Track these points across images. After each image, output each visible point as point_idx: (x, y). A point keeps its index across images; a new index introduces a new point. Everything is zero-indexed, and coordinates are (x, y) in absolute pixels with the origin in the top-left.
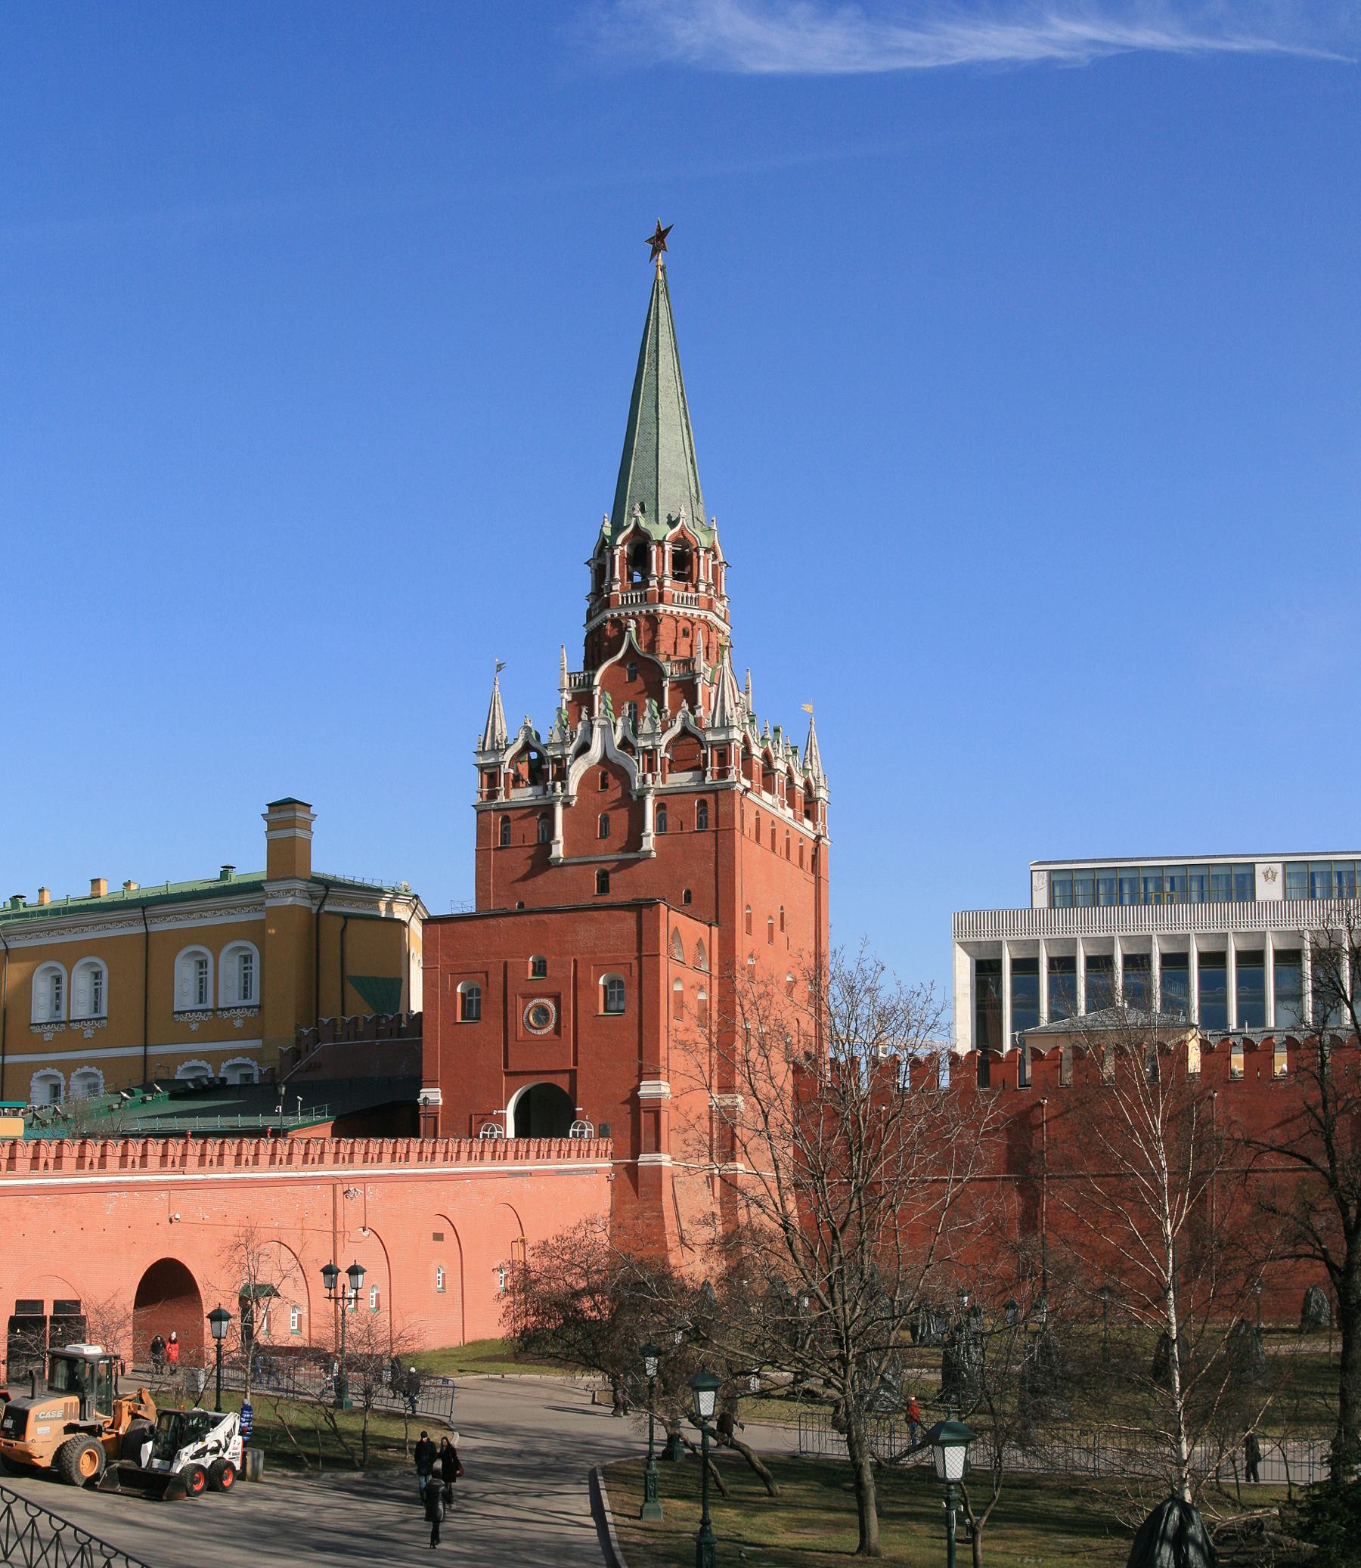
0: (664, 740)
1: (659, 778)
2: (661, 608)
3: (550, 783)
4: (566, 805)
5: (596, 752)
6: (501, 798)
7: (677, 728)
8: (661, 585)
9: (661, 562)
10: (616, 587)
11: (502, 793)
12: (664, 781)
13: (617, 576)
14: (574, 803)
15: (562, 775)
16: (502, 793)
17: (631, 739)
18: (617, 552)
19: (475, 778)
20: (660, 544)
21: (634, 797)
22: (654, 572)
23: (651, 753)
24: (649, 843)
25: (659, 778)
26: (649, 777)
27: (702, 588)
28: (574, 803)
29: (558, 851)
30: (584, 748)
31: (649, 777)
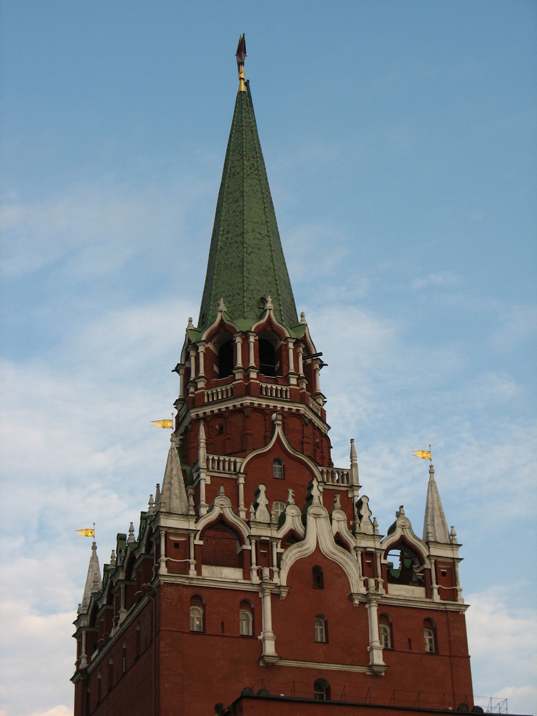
0: (384, 547)
1: (381, 586)
2: (302, 409)
3: (254, 566)
4: (275, 596)
6: (193, 573)
9: (294, 363)
10: (253, 375)
11: (192, 567)
13: (252, 363)
14: (284, 595)
16: (192, 567)
17: (346, 535)
18: (252, 339)
21: (357, 602)
23: (369, 557)
24: (378, 658)
25: (381, 586)
26: (372, 582)
28: (284, 595)
29: (270, 648)
31: (372, 582)
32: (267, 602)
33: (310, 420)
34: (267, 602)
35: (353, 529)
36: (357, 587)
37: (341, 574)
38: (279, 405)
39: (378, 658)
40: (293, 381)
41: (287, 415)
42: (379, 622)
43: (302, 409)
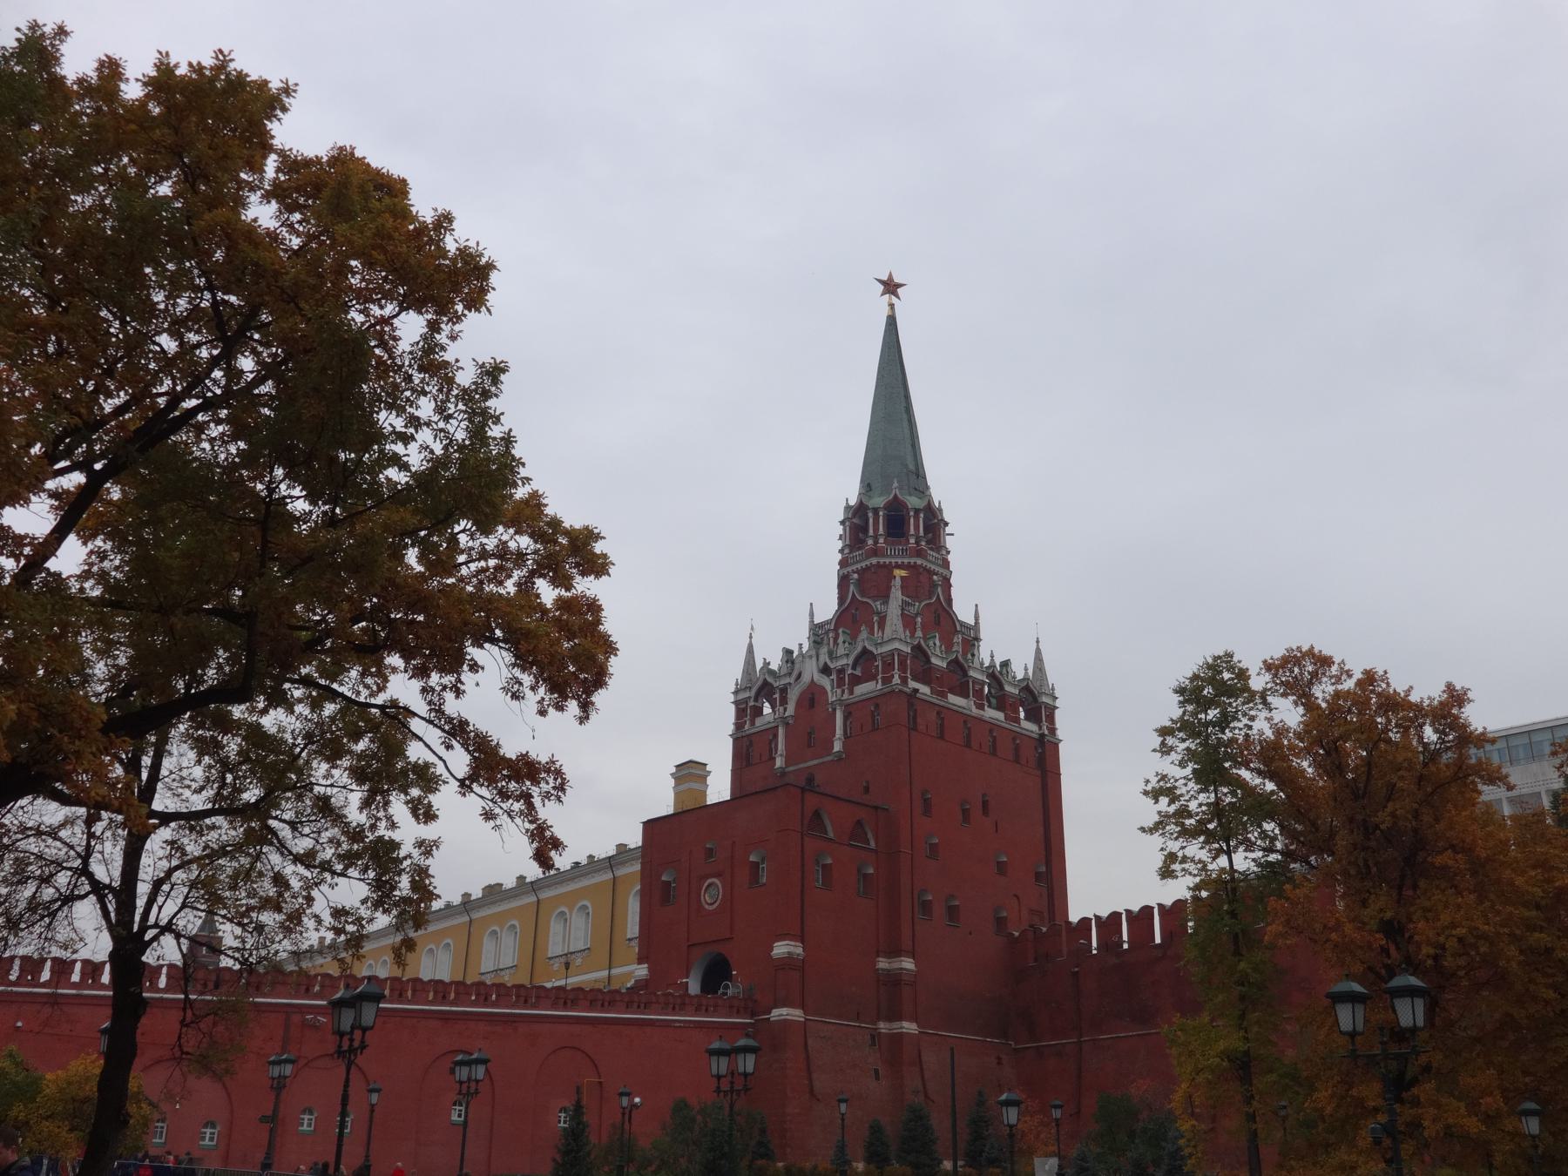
0: (850, 662)
2: (874, 561)
5: (806, 678)
7: (859, 649)
8: (876, 542)
12: (851, 693)
15: (784, 701)
19: (730, 713)
20: (876, 511)
22: (871, 532)
24: (837, 747)
27: (912, 541)
29: (779, 762)
30: (799, 676)
32: (781, 731)
33: (884, 566)
34: (781, 731)
35: (830, 653)
36: (832, 698)
37: (823, 690)
38: (859, 566)
39: (837, 747)
40: (870, 542)
41: (862, 572)
42: (846, 719)
43: (874, 561)
